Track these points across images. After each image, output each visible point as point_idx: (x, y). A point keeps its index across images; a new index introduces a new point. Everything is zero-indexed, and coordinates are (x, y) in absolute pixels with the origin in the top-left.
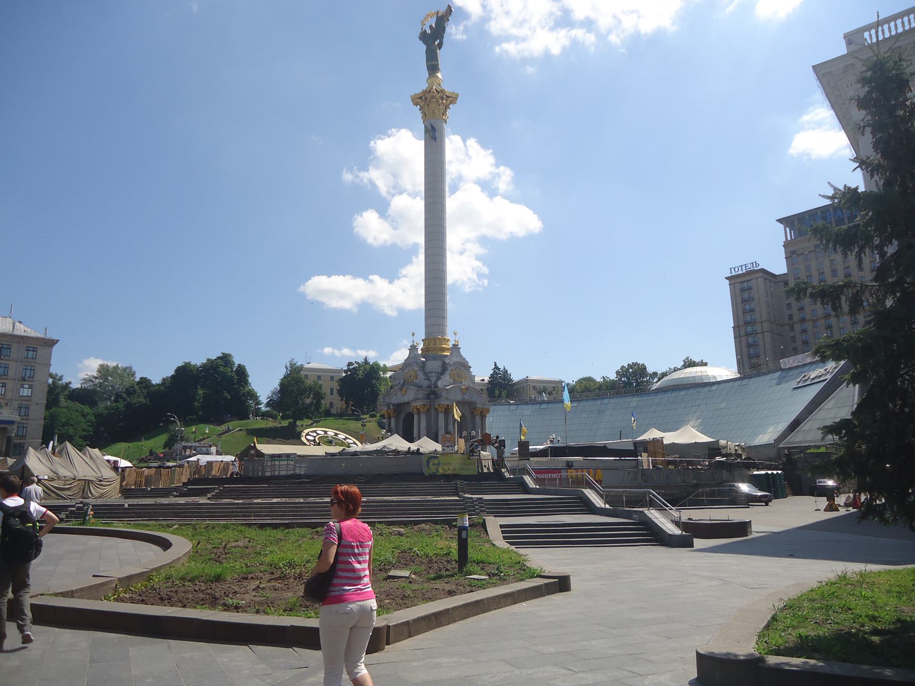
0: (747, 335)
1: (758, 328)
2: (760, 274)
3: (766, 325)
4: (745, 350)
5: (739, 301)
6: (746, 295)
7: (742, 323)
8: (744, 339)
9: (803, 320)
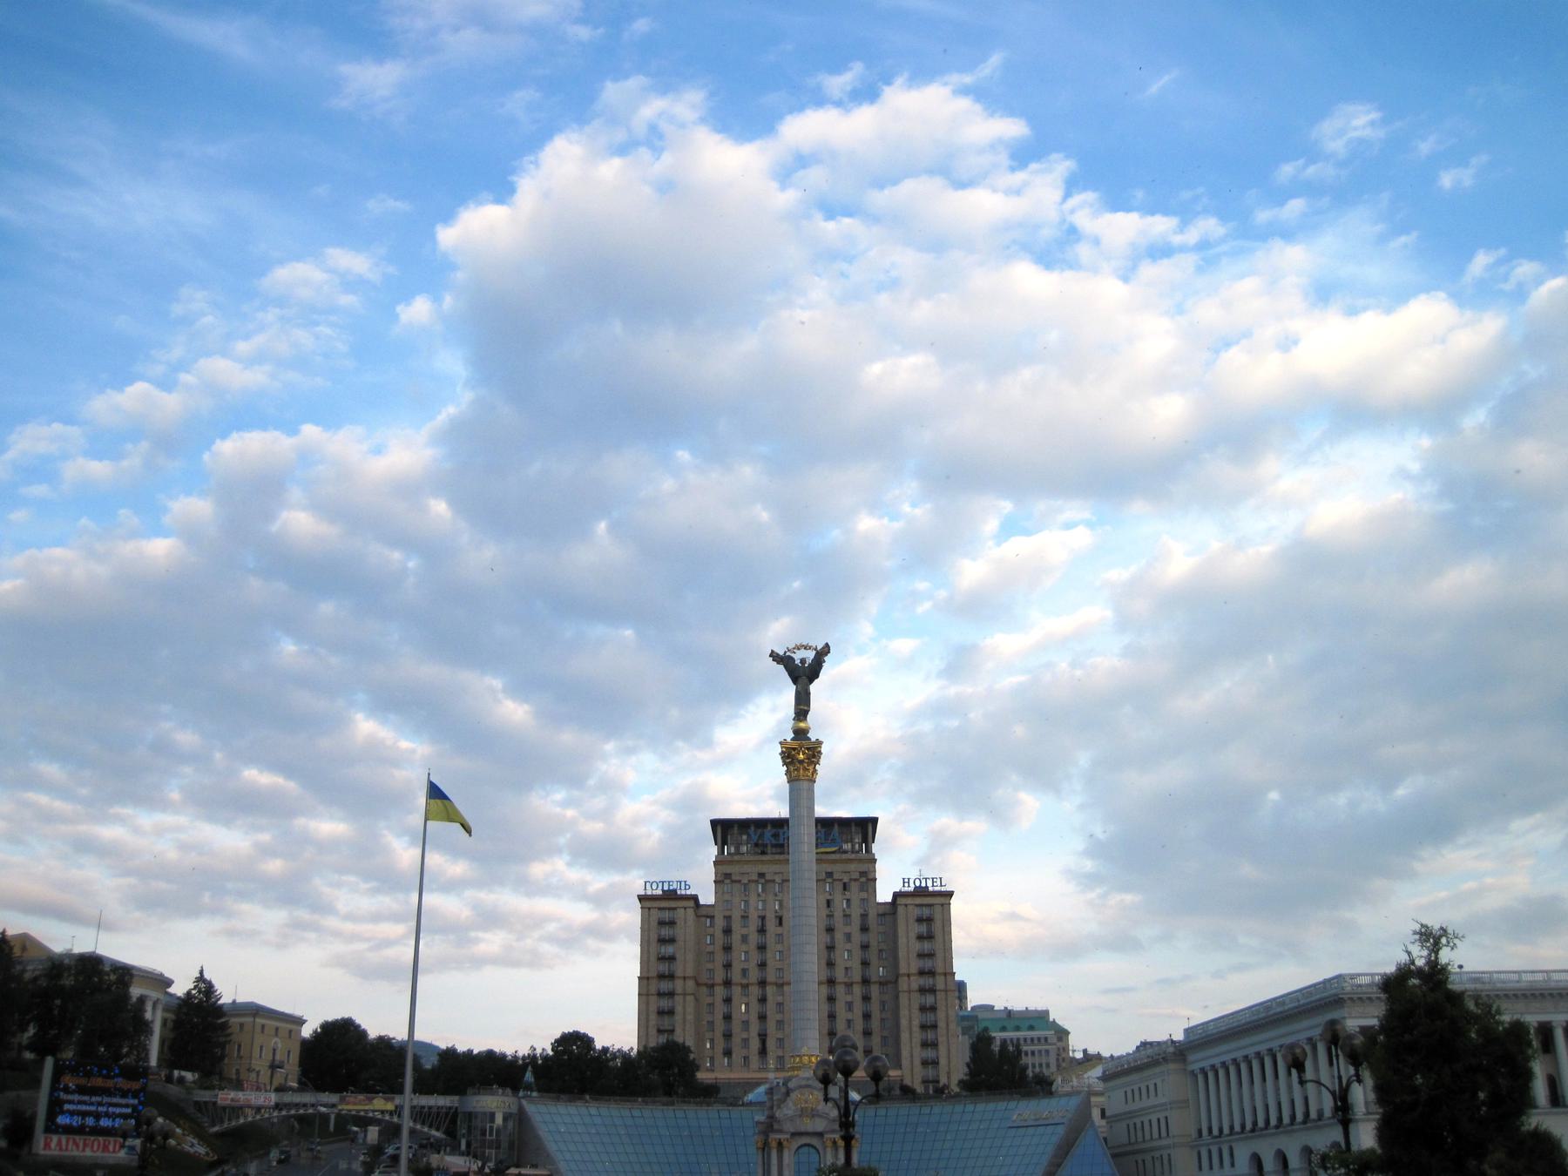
0: (660, 994)
1: (679, 985)
2: (692, 903)
3: (690, 984)
4: (653, 1017)
5: (654, 937)
6: (666, 932)
7: (653, 974)
8: (653, 999)
9: (727, 983)
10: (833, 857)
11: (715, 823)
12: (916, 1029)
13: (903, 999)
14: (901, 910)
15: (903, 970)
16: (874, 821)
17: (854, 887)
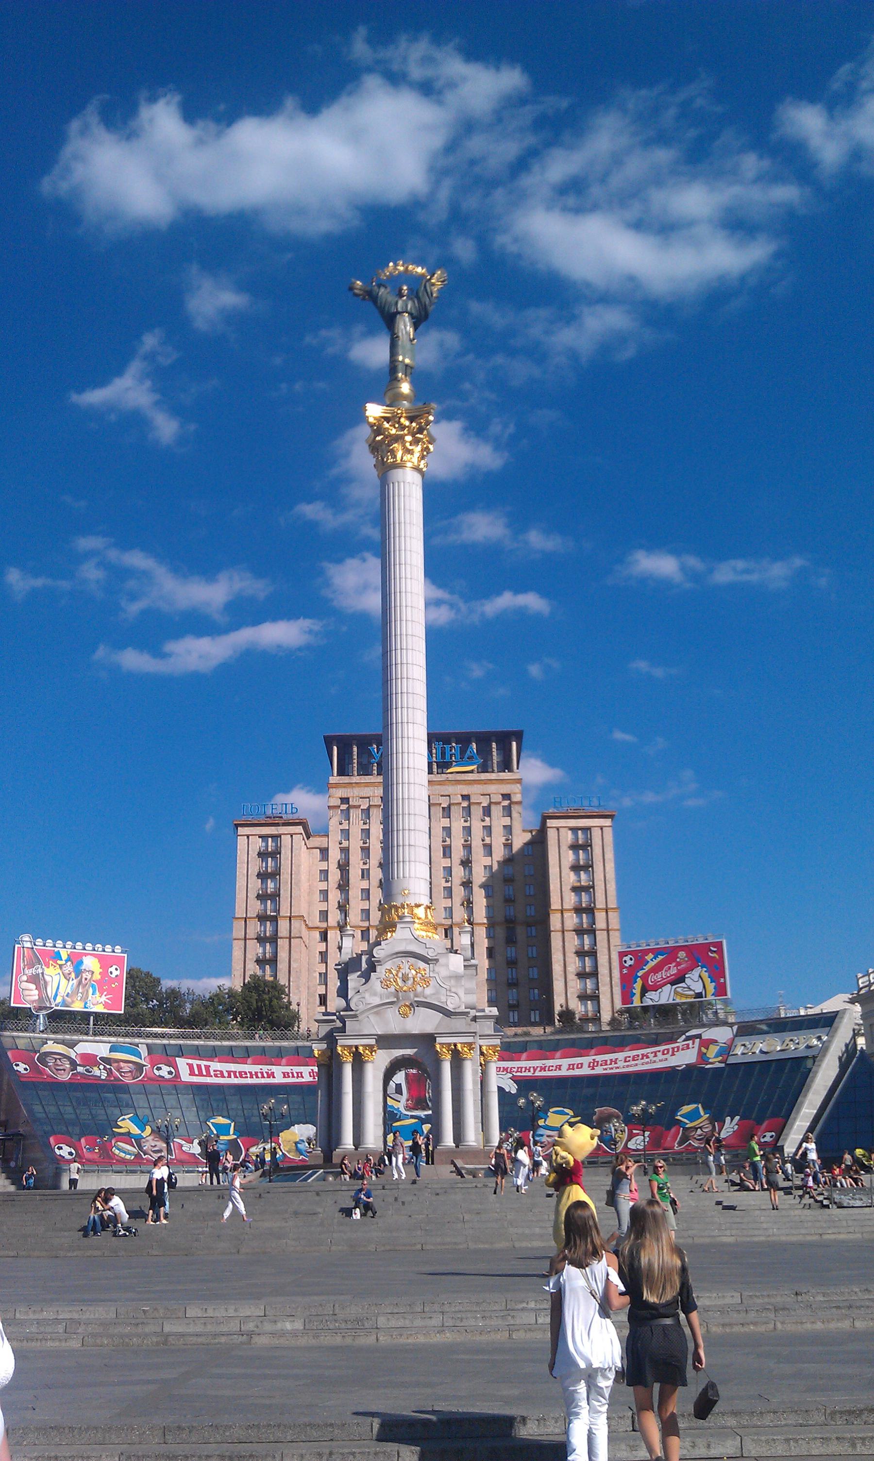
10: (470, 777)
11: (329, 741)
12: (572, 977)
13: (556, 941)
14: (552, 835)
15: (555, 904)
16: (518, 736)
17: (496, 811)
